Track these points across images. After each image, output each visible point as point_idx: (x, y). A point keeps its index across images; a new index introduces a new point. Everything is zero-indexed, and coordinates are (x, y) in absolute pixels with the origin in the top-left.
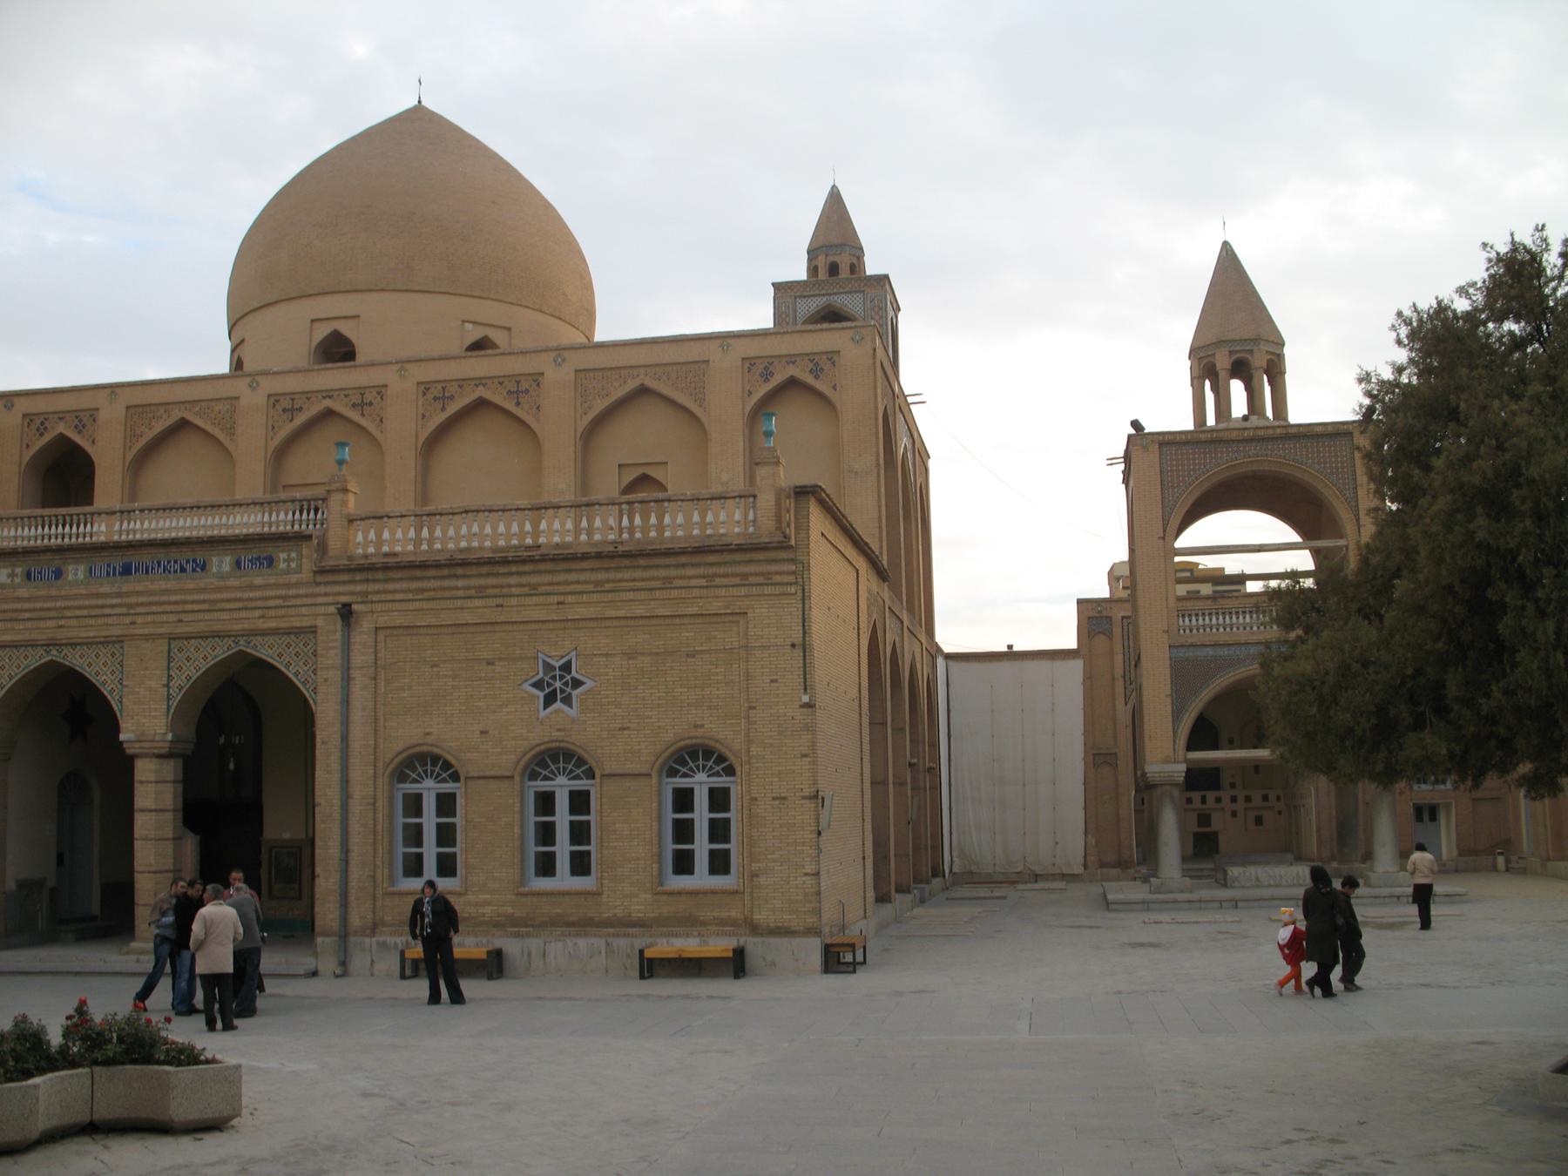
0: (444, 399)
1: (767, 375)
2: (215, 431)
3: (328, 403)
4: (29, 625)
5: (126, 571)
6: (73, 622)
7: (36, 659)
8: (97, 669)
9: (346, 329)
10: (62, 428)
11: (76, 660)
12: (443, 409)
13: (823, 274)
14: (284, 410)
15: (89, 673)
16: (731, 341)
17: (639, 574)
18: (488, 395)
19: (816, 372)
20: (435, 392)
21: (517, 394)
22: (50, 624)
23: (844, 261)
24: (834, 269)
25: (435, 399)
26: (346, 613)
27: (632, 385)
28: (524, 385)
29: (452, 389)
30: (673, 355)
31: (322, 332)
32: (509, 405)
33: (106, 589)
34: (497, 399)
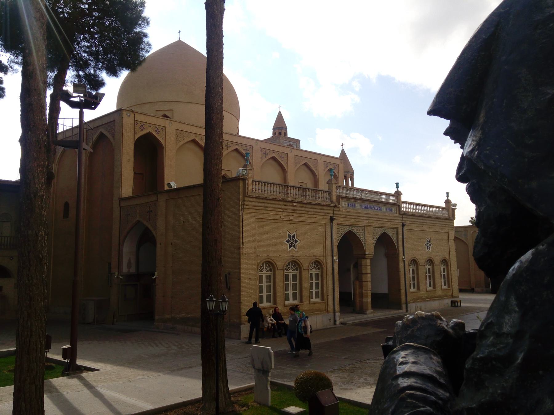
0: (266, 154)
1: (327, 167)
3: (237, 147)
4: (348, 219)
5: (367, 208)
6: (357, 220)
7: (346, 230)
8: (359, 233)
10: (150, 130)
11: (355, 230)
13: (277, 134)
15: (358, 234)
17: (438, 223)
19: (335, 168)
20: (264, 151)
22: (353, 220)
23: (283, 132)
24: (280, 133)
26: (403, 225)
27: (304, 162)
29: (267, 152)
30: (105, 121)
33: (365, 212)
34: (277, 158)
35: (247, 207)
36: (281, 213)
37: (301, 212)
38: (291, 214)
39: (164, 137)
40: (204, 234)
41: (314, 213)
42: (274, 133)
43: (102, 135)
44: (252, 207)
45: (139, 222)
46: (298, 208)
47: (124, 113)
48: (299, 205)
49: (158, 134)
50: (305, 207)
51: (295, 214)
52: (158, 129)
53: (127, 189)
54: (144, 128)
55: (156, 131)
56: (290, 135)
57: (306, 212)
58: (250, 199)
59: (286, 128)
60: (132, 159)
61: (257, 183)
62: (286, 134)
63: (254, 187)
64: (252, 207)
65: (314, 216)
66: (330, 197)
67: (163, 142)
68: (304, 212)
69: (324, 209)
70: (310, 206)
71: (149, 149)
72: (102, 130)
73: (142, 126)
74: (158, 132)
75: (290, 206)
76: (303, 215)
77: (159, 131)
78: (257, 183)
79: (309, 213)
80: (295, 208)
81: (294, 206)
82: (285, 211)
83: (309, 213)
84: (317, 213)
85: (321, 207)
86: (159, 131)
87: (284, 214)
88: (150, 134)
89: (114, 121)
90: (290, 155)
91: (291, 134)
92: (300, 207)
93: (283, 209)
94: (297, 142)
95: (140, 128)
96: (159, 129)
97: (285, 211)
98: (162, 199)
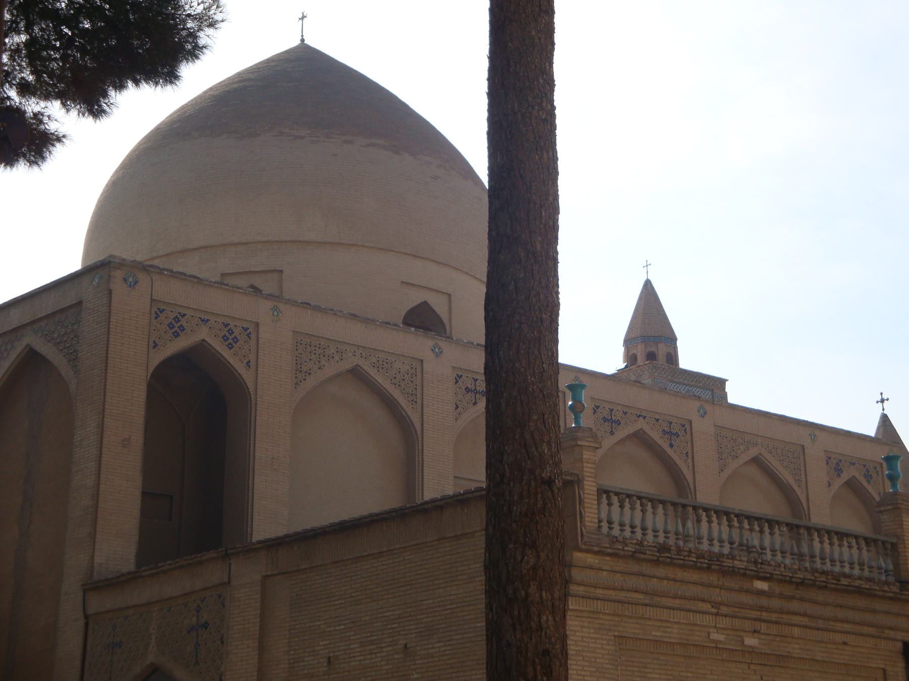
1: (839, 471)
2: (396, 394)
9: (438, 305)
10: (203, 334)
12: (612, 433)
14: (468, 390)
16: (817, 432)
18: (647, 429)
19: (868, 477)
21: (669, 434)
23: (662, 350)
24: (651, 356)
25: (605, 420)
28: (676, 428)
31: (415, 298)
32: (665, 445)
34: (656, 436)
35: (581, 590)
36: (708, 620)
37: (786, 618)
38: (747, 625)
39: (252, 357)
40: (494, 632)
41: (839, 626)
42: (631, 358)
43: (32, 358)
44: (600, 592)
45: (154, 669)
46: (775, 603)
47: (118, 275)
48: (778, 589)
49: (230, 346)
50: (802, 599)
51: (763, 627)
52: (231, 332)
53: (116, 543)
54: (182, 328)
55: (225, 338)
56: (688, 360)
57: (805, 621)
58: (591, 559)
59: (670, 339)
60: (138, 439)
61: (615, 500)
62: (672, 358)
63: (604, 515)
64: (600, 592)
65: (839, 638)
66: (897, 565)
67: (247, 376)
68: (797, 619)
69: (874, 611)
70: (820, 596)
71: (200, 409)
72: (32, 340)
73: (177, 319)
74: (230, 340)
75: (740, 591)
76: (796, 631)
77: (236, 340)
78: (615, 500)
79: (821, 624)
80: (764, 601)
81: (760, 593)
82: (724, 610)
83: (821, 624)
84: (847, 627)
85: (861, 602)
86: (236, 340)
87: (724, 622)
88: (202, 348)
89: (80, 303)
90: (702, 426)
91: (688, 360)
92: (781, 596)
93: (716, 605)
94: (718, 384)
95: (171, 326)
96: (237, 332)
97: (724, 610)
98: (247, 575)
